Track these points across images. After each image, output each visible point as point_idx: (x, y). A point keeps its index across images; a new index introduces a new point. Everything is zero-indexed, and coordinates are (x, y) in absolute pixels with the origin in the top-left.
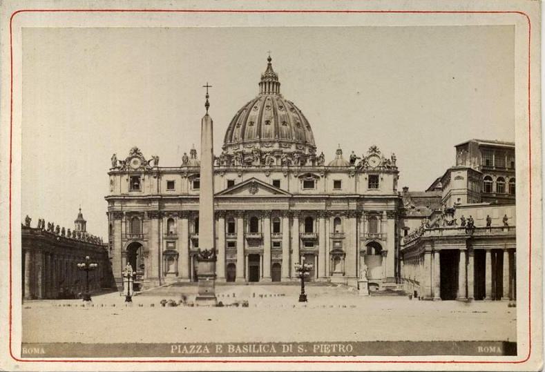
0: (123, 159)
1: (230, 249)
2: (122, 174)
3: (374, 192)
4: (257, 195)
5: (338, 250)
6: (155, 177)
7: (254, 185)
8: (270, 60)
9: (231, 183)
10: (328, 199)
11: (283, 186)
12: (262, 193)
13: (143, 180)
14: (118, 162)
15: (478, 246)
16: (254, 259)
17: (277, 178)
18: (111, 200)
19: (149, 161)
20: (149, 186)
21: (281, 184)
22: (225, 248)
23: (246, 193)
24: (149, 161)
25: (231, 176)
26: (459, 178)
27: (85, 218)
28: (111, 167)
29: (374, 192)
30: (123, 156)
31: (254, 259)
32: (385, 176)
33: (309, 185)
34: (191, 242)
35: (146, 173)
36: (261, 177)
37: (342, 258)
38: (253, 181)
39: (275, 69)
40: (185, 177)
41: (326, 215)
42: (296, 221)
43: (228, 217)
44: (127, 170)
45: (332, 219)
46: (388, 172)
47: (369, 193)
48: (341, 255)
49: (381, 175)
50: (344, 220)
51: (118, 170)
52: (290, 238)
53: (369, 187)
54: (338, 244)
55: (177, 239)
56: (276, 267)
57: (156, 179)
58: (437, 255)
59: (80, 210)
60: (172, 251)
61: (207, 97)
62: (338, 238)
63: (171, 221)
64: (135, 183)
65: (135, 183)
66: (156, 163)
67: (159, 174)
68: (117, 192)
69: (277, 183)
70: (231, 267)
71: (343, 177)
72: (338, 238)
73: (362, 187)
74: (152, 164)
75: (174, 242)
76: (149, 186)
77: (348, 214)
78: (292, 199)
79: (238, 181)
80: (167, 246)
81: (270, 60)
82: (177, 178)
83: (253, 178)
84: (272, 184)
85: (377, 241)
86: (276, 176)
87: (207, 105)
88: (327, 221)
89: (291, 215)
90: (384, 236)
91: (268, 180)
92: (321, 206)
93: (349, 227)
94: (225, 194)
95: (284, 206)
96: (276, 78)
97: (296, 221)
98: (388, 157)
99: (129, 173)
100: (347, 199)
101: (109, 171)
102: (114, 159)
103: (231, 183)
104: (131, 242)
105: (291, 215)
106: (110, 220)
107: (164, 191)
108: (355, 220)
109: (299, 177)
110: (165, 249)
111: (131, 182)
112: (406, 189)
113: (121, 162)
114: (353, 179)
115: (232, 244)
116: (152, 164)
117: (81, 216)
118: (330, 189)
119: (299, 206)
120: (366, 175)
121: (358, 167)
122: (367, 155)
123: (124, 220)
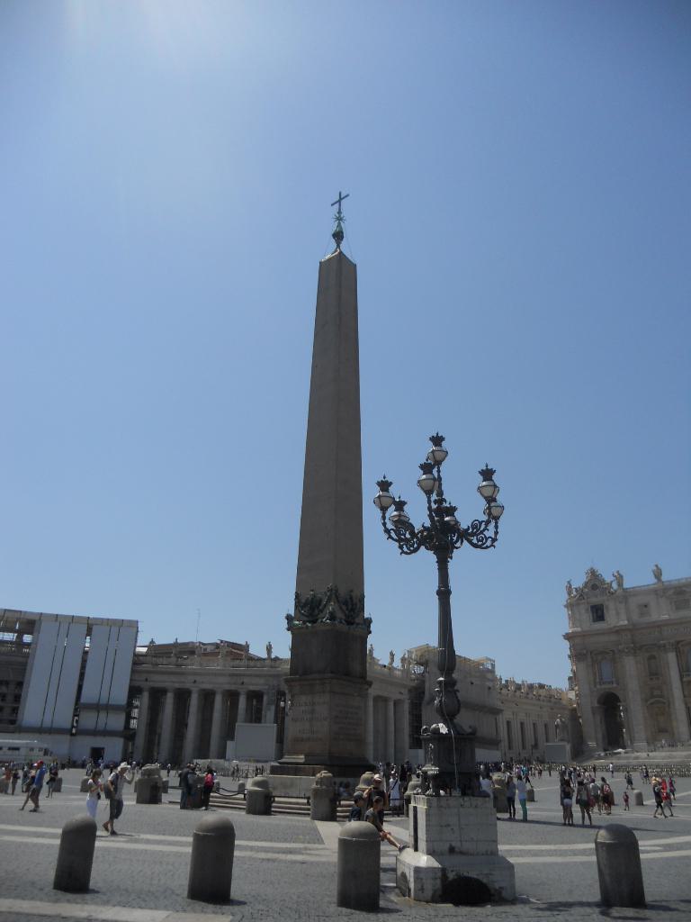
2: (578, 604)
6: (620, 602)
18: (568, 637)
20: (616, 618)
28: (567, 597)
30: (579, 581)
61: (339, 219)
63: (652, 657)
64: (598, 613)
65: (598, 613)
66: (620, 584)
67: (627, 595)
68: (579, 629)
74: (615, 586)
76: (616, 618)
87: (338, 236)
116: (615, 586)
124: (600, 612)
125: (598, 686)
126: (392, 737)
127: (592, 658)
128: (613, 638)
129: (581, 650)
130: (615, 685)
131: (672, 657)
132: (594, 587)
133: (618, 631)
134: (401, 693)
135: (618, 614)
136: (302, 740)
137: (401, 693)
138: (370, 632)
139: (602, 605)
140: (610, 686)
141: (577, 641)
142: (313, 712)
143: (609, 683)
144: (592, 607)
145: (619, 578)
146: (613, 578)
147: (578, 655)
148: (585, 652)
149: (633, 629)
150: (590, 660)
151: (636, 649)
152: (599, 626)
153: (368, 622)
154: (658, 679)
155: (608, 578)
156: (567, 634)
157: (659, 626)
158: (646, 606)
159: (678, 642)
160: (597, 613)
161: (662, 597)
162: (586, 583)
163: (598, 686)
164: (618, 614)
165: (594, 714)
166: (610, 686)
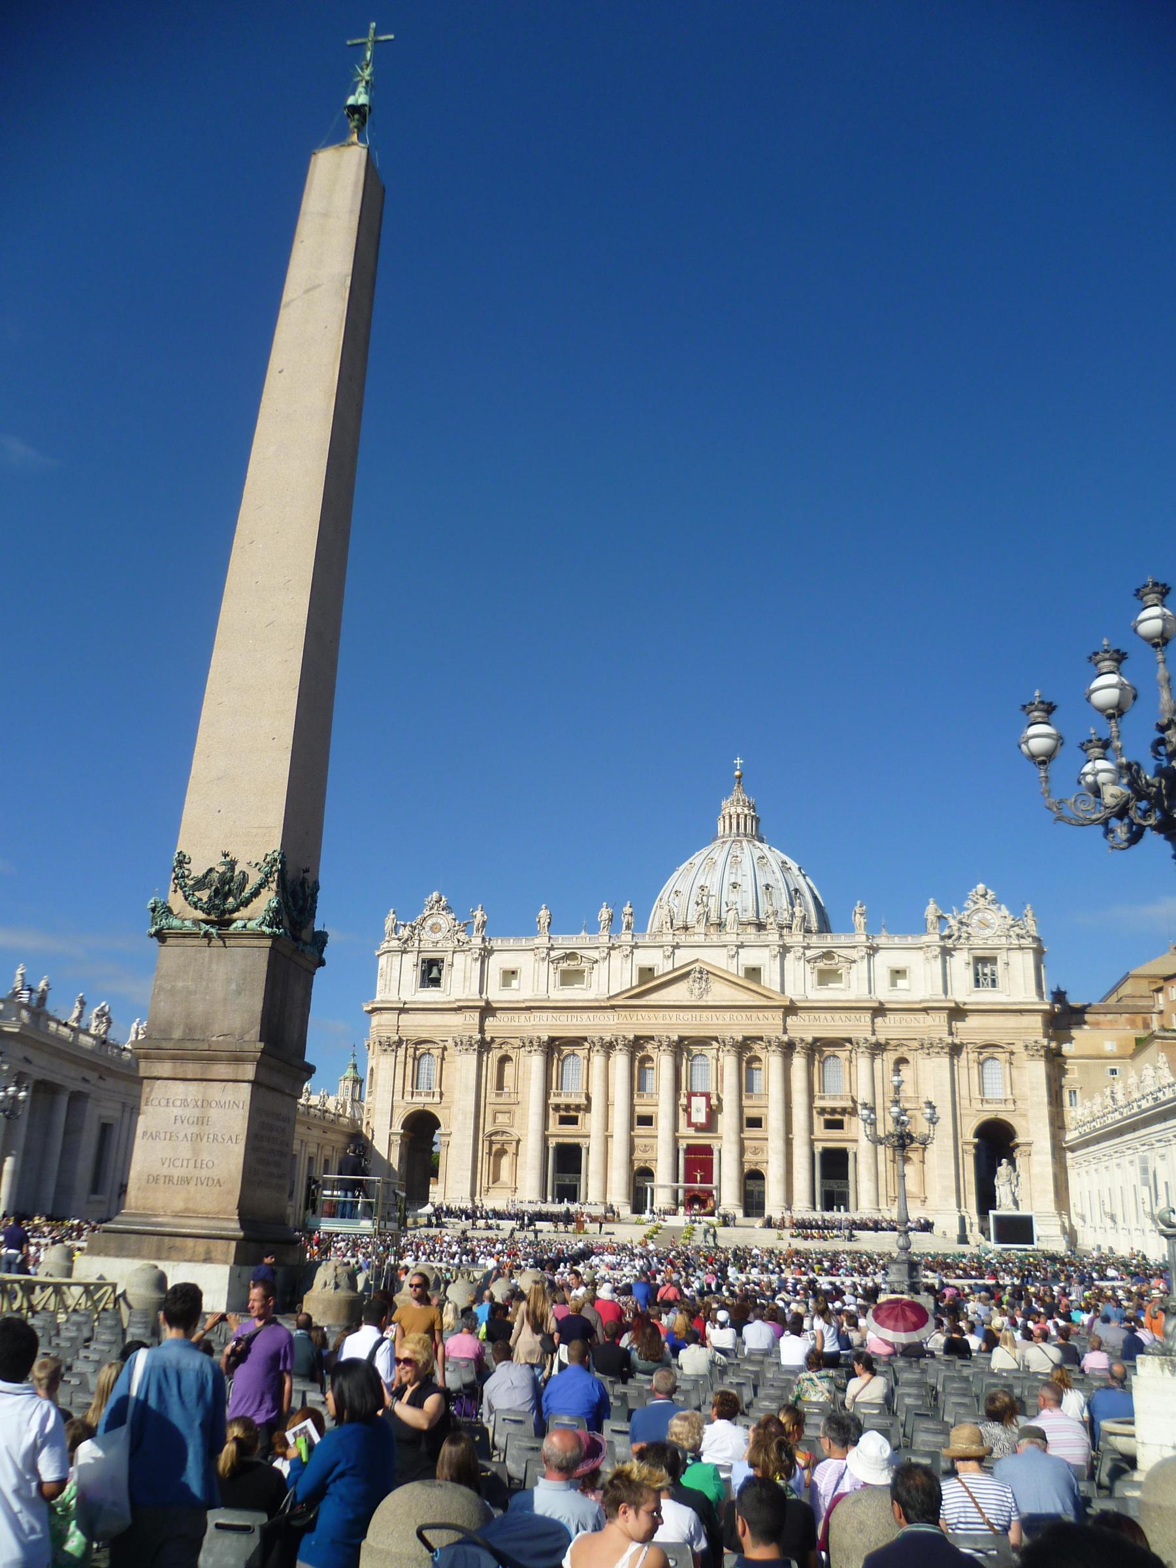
3: (986, 997)
4: (709, 1000)
7: (705, 974)
9: (646, 973)
11: (771, 978)
12: (720, 993)
13: (452, 965)
17: (753, 963)
21: (765, 976)
23: (677, 994)
25: (644, 958)
29: (986, 997)
31: (698, 1161)
32: (1016, 956)
33: (826, 977)
34: (551, 1112)
36: (716, 959)
38: (697, 966)
40: (543, 959)
45: (890, 1057)
46: (1021, 948)
49: (1002, 957)
53: (977, 986)
56: (752, 1180)
69: (753, 973)
70: (640, 1178)
73: (963, 991)
77: (927, 1047)
78: (791, 1009)
80: (495, 1118)
83: (697, 960)
84: (742, 974)
85: (1002, 1116)
86: (750, 958)
88: (878, 1062)
91: (734, 968)
92: (859, 1027)
95: (769, 1025)
103: (646, 973)
104: (412, 1109)
107: (496, 994)
108: (946, 1060)
110: (489, 1129)
111: (423, 972)
118: (884, 993)
123: (401, 1059)
124: (434, 974)
125: (408, 1098)
126: (54, 1163)
130: (437, 1099)
131: (536, 1062)
134: (85, 1080)
136: (169, 1179)
137: (85, 1080)
138: (322, 963)
140: (429, 1100)
142: (202, 1121)
143: (428, 1094)
144: (423, 961)
149: (487, 1010)
150: (401, 1052)
152: (431, 995)
153: (321, 939)
158: (513, 973)
163: (408, 1098)
166: (429, 1100)
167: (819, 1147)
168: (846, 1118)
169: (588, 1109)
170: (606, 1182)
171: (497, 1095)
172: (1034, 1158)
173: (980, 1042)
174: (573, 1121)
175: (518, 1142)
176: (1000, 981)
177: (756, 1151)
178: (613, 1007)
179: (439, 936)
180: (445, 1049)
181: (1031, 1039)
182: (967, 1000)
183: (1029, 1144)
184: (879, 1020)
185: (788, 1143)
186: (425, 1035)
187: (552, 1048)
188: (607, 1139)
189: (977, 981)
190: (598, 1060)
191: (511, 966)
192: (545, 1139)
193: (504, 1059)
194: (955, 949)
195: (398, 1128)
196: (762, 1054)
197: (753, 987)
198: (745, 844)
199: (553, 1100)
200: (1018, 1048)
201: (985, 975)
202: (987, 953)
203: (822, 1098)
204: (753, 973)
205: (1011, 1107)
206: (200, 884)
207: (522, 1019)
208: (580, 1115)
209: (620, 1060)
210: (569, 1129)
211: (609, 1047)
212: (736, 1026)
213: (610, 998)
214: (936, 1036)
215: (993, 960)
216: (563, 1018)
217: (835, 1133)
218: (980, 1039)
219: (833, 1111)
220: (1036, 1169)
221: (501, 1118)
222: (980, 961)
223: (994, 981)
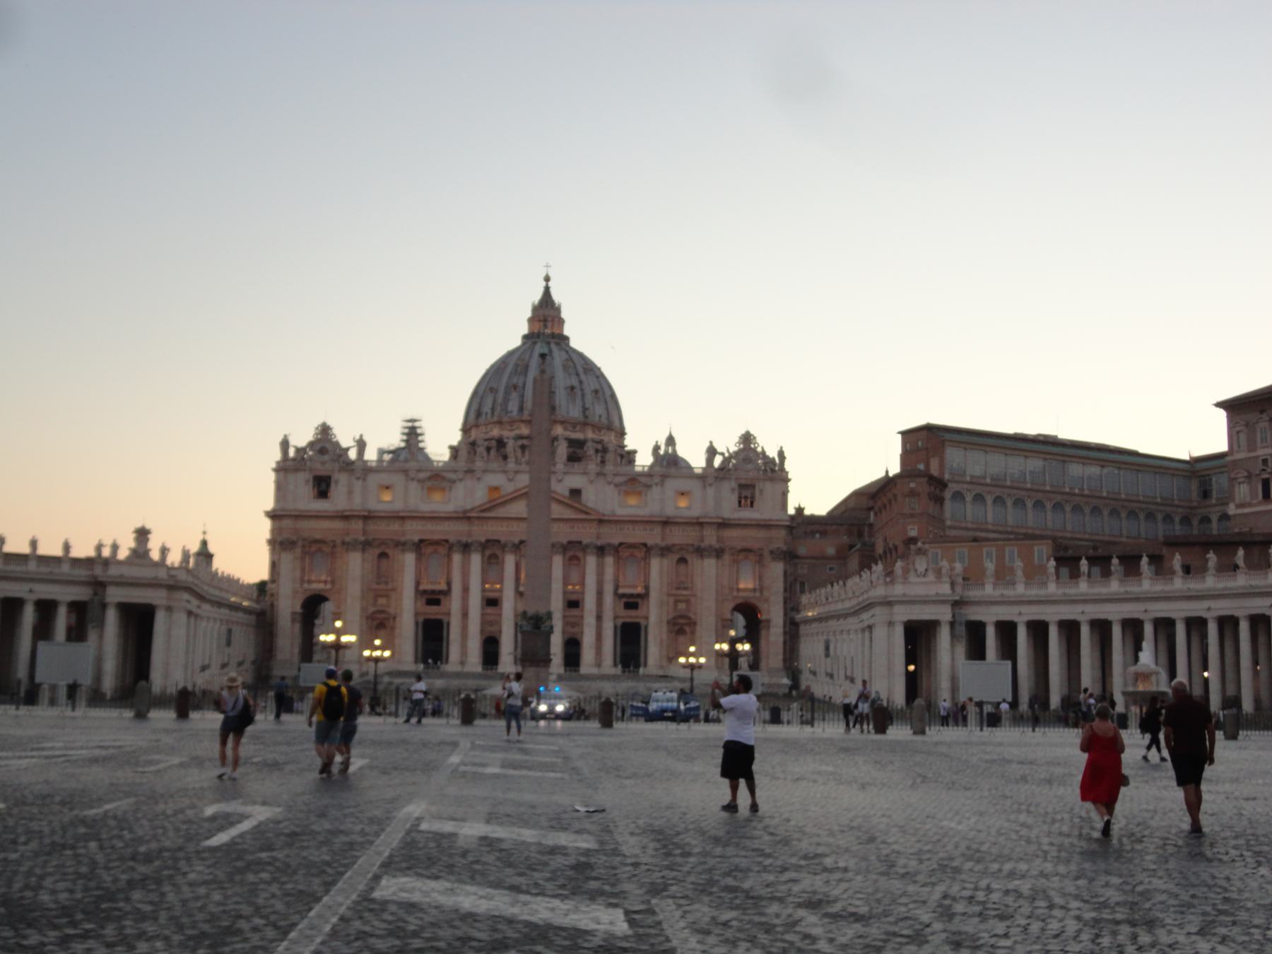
0: (302, 443)
1: (490, 610)
2: (297, 470)
5: (681, 617)
6: (358, 478)
8: (547, 279)
10: (666, 523)
14: (292, 453)
15: (975, 614)
16: (534, 628)
18: (273, 516)
19: (348, 449)
21: (584, 494)
22: (483, 608)
24: (348, 449)
26: (913, 494)
27: (212, 548)
28: (277, 456)
29: (747, 514)
30: (302, 437)
32: (768, 487)
35: (341, 470)
37: (687, 629)
39: (557, 296)
41: (665, 551)
42: (609, 560)
43: (488, 553)
44: (308, 464)
46: (771, 479)
47: (736, 515)
48: (689, 624)
49: (759, 486)
50: (694, 561)
51: (289, 467)
52: (600, 593)
54: (682, 606)
55: (394, 590)
57: (360, 482)
58: (899, 632)
59: (204, 533)
60: (383, 612)
62: (681, 591)
63: (383, 555)
64: (322, 486)
65: (322, 486)
71: (694, 486)
72: (681, 591)
73: (728, 508)
75: (387, 596)
77: (701, 552)
79: (509, 488)
81: (547, 279)
82: (397, 479)
84: (567, 493)
85: (753, 601)
89: (601, 551)
90: (766, 593)
92: (653, 537)
93: (707, 572)
94: (483, 511)
95: (587, 534)
96: (558, 310)
97: (609, 560)
98: (772, 453)
99: (311, 470)
100: (699, 524)
101: (274, 466)
102: (285, 444)
104: (308, 594)
105: (601, 551)
106: (273, 551)
109: (616, 485)
112: (800, 510)
113: (298, 450)
114: (710, 492)
115: (492, 602)
116: (353, 455)
117: (204, 543)
119: (614, 536)
120: (734, 484)
121: (721, 469)
122: (733, 449)
124: (323, 486)
125: (306, 586)
127: (303, 546)
128: (338, 525)
129: (289, 534)
131: (410, 559)
132: (322, 451)
133: (345, 517)
135: (350, 493)
139: (330, 477)
141: (287, 523)
145: (361, 445)
146: (353, 444)
147: (279, 544)
148: (295, 538)
149: (368, 517)
150: (298, 550)
151: (366, 545)
152: (321, 505)
154: (386, 583)
155: (345, 438)
156: (274, 510)
157: (400, 518)
159: (421, 541)
160: (319, 485)
161: (413, 479)
162: (311, 444)
164: (350, 493)
165: (293, 621)
166: (321, 586)
167: (620, 622)
168: (639, 600)
169: (447, 592)
170: (464, 651)
171: (378, 583)
172: (772, 630)
173: (739, 548)
174: (437, 602)
175: (394, 618)
176: (755, 504)
177: (574, 625)
178: (469, 518)
179: (326, 458)
180: (334, 546)
181: (774, 546)
182: (732, 516)
183: (768, 621)
184: (667, 530)
185: (599, 618)
186: (318, 536)
187: (420, 546)
188: (465, 615)
189: (740, 502)
190: (457, 558)
191: (386, 483)
192: (417, 614)
193: (383, 555)
194: (723, 479)
195: (298, 609)
196: (580, 554)
197: (577, 505)
198: (553, 346)
199: (422, 587)
200: (766, 553)
201: (746, 498)
202: (749, 482)
203: (625, 587)
204: (576, 493)
205: (758, 594)
206: (531, 618)
207: (396, 526)
208: (442, 597)
209: (476, 560)
210: (434, 609)
211: (466, 548)
212: (563, 534)
213: (465, 512)
214: (706, 543)
215: (753, 486)
216: (430, 526)
217: (632, 613)
218: (739, 545)
219: (632, 596)
220: (772, 638)
221: (382, 601)
222: (741, 487)
223: (752, 503)
